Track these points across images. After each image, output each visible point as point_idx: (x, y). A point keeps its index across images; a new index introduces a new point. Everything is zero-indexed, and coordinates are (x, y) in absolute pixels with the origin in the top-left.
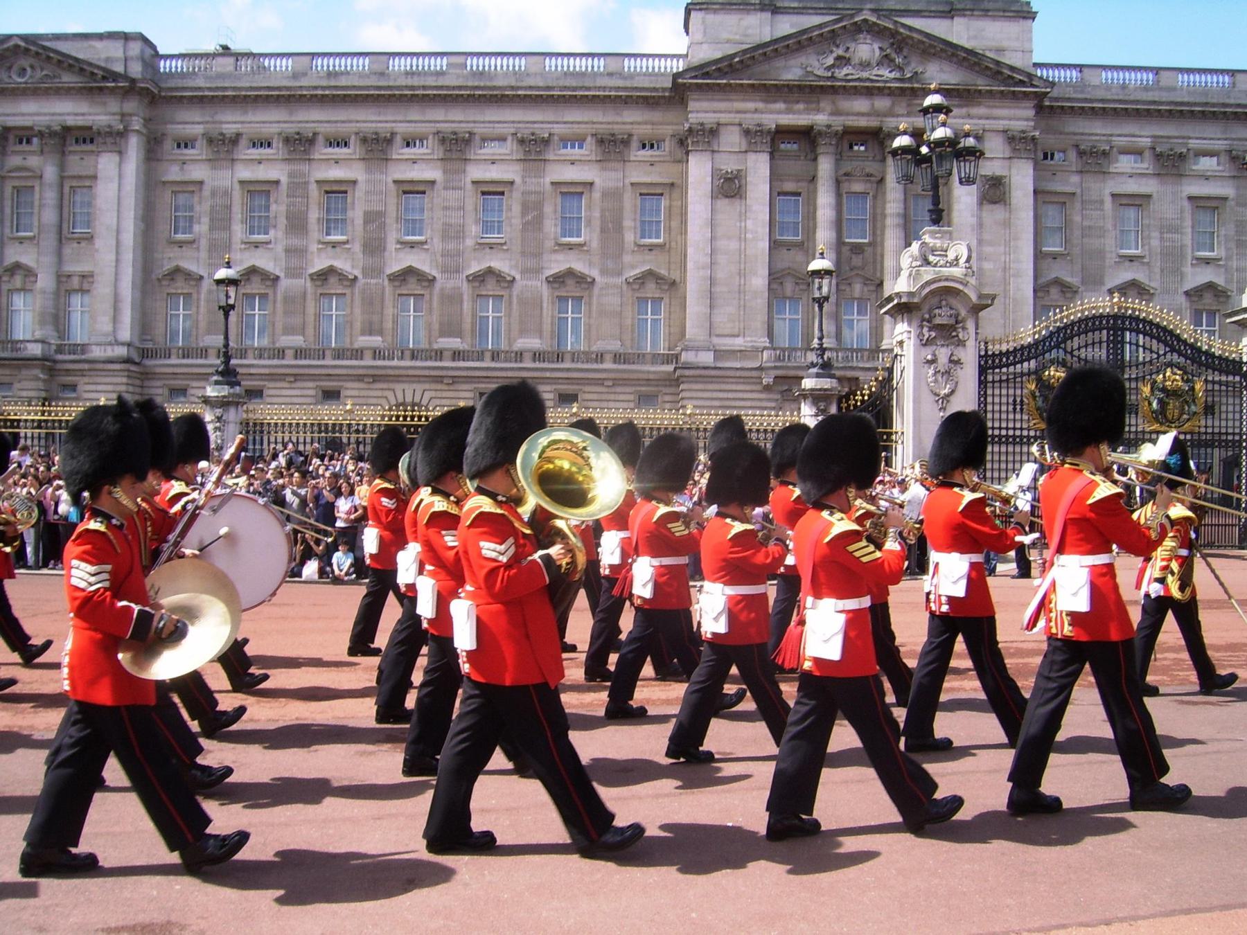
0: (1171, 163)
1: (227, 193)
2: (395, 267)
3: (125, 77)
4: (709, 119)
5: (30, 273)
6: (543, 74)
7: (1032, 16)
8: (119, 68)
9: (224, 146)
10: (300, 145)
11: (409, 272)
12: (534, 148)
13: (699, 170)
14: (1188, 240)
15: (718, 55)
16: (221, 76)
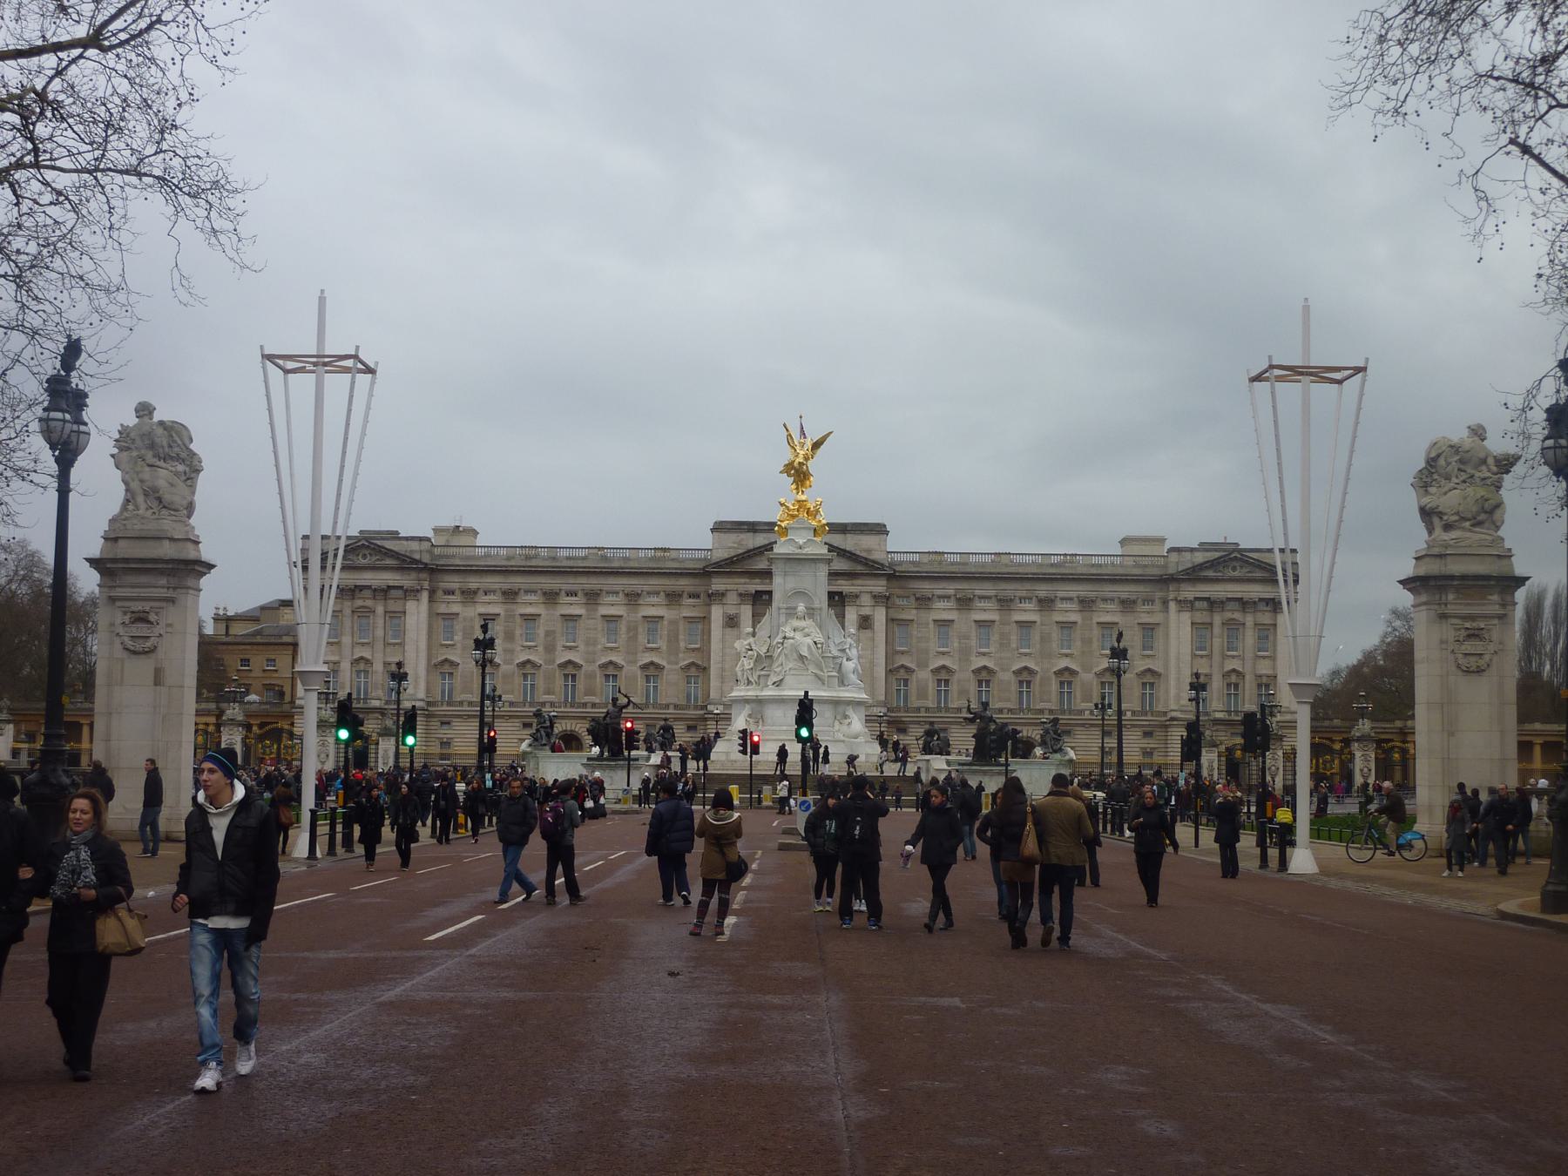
0: (965, 603)
1: (472, 620)
2: (563, 660)
3: (419, 562)
4: (721, 588)
5: (367, 661)
6: (638, 559)
7: (887, 533)
8: (417, 557)
9: (469, 595)
10: (510, 595)
11: (570, 662)
12: (633, 598)
13: (717, 613)
14: (973, 643)
15: (726, 556)
16: (468, 558)
